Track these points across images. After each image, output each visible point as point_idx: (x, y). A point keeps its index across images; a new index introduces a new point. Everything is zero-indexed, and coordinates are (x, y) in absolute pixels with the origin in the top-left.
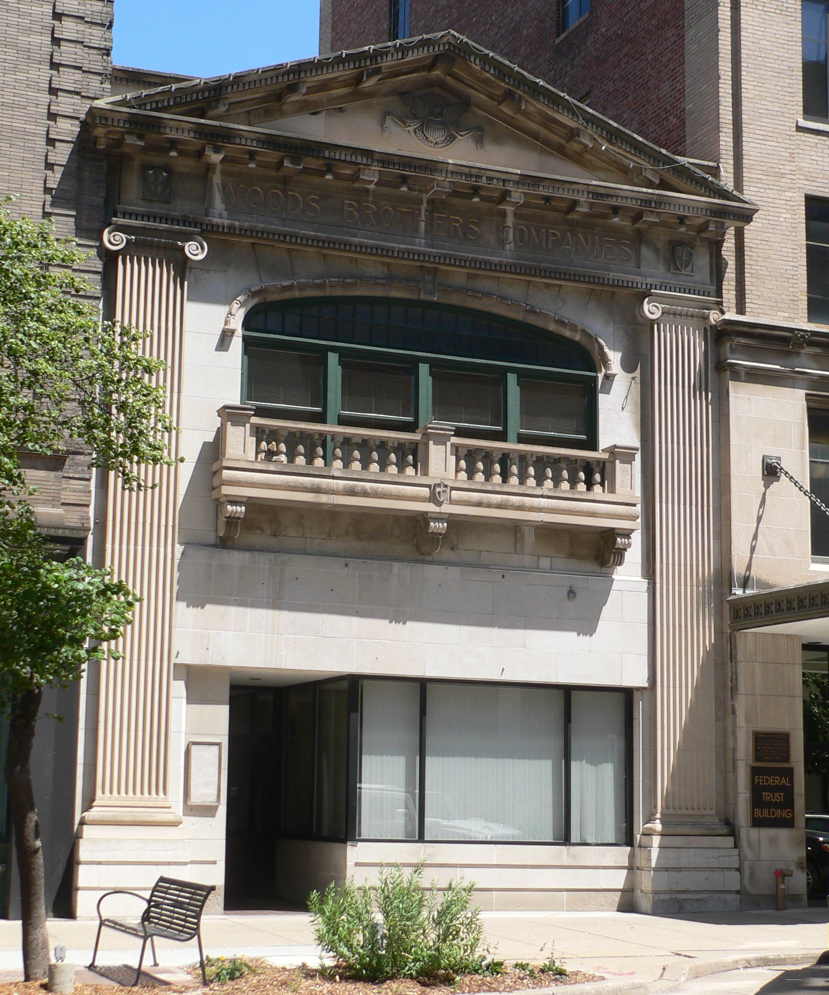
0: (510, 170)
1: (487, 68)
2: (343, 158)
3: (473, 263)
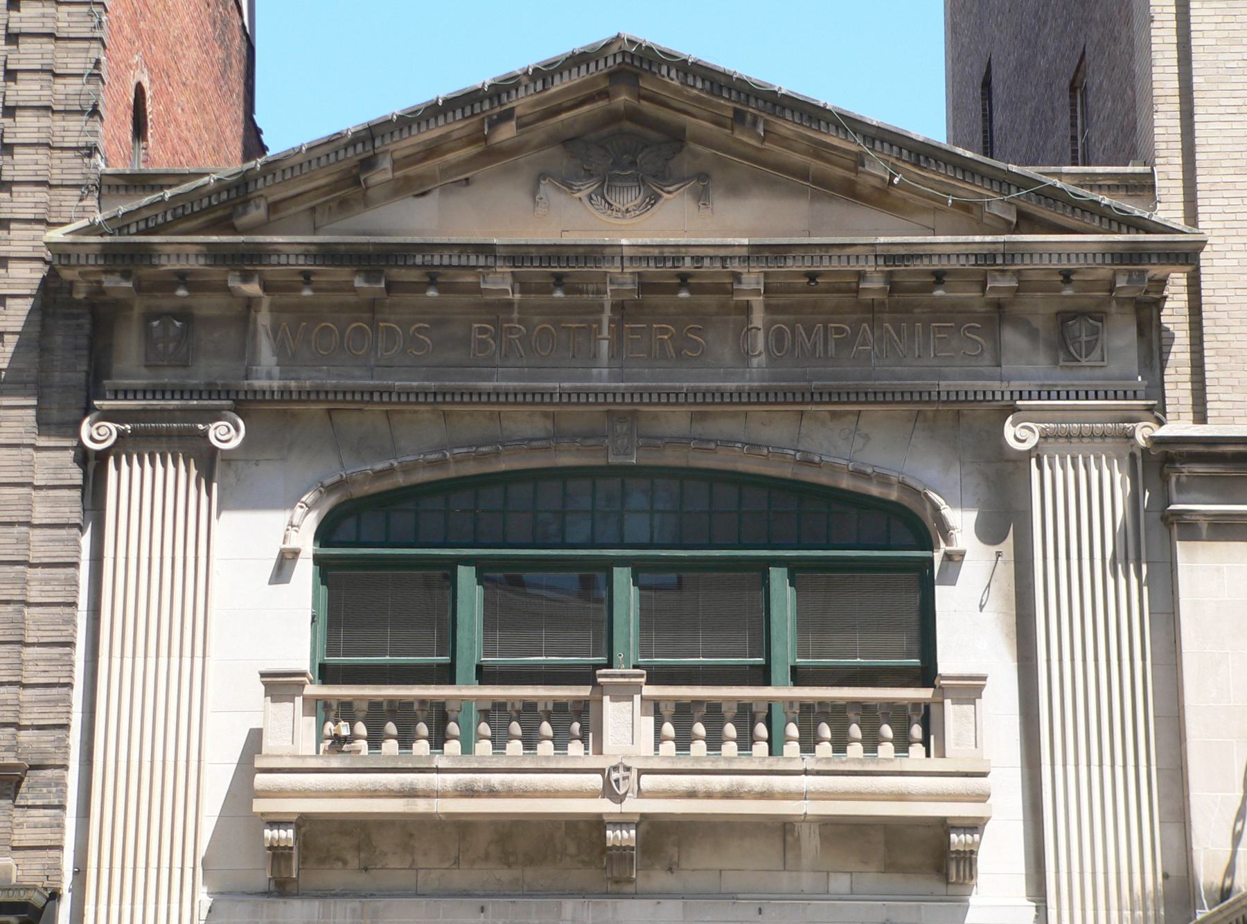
0: (730, 241)
1: (690, 81)
2: (446, 261)
3: (691, 396)
